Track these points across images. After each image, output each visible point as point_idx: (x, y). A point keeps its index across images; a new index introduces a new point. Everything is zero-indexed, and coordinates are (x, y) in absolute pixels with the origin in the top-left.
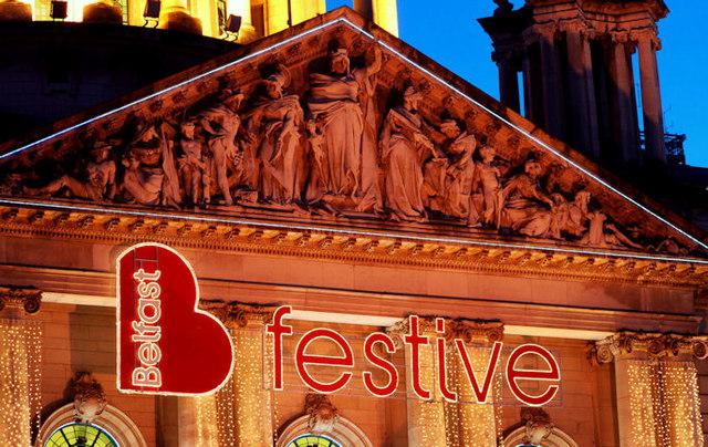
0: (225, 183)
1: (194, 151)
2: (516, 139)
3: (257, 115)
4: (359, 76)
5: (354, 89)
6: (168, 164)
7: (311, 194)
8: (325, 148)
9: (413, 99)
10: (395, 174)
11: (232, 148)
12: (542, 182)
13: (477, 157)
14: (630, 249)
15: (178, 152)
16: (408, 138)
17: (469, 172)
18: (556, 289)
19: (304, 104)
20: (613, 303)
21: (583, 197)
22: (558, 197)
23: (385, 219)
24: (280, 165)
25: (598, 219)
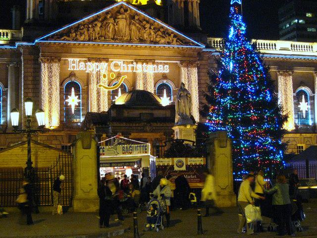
0: (97, 36)
1: (91, 30)
2: (158, 24)
3: (105, 22)
4: (125, 14)
5: (124, 16)
6: (86, 33)
7: (115, 37)
8: (118, 28)
9: (137, 18)
10: (133, 33)
11: (99, 29)
12: (164, 33)
13: (150, 28)
14: (182, 45)
15: (88, 30)
16: (135, 25)
17: (148, 31)
18: (167, 53)
19: (114, 20)
20: (180, 56)
21: (172, 35)
22: (167, 35)
23: (130, 41)
24: (109, 32)
25: (175, 39)
